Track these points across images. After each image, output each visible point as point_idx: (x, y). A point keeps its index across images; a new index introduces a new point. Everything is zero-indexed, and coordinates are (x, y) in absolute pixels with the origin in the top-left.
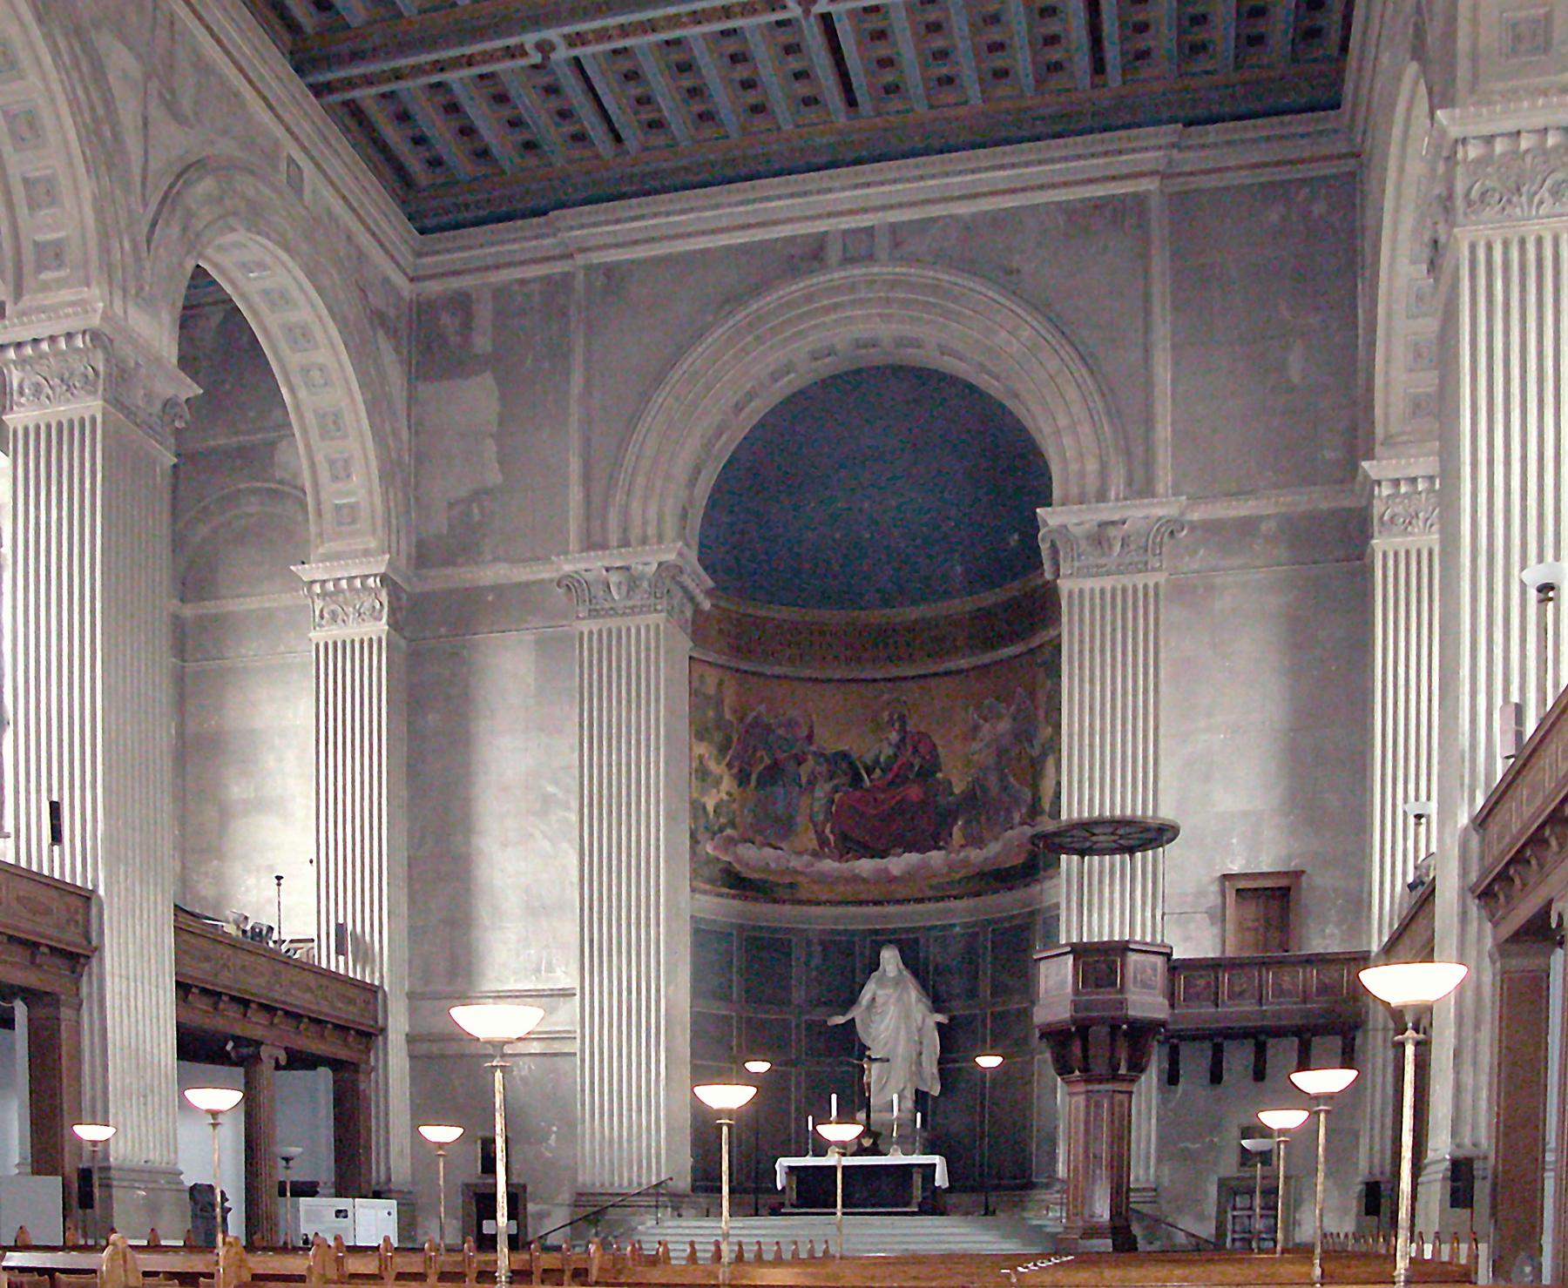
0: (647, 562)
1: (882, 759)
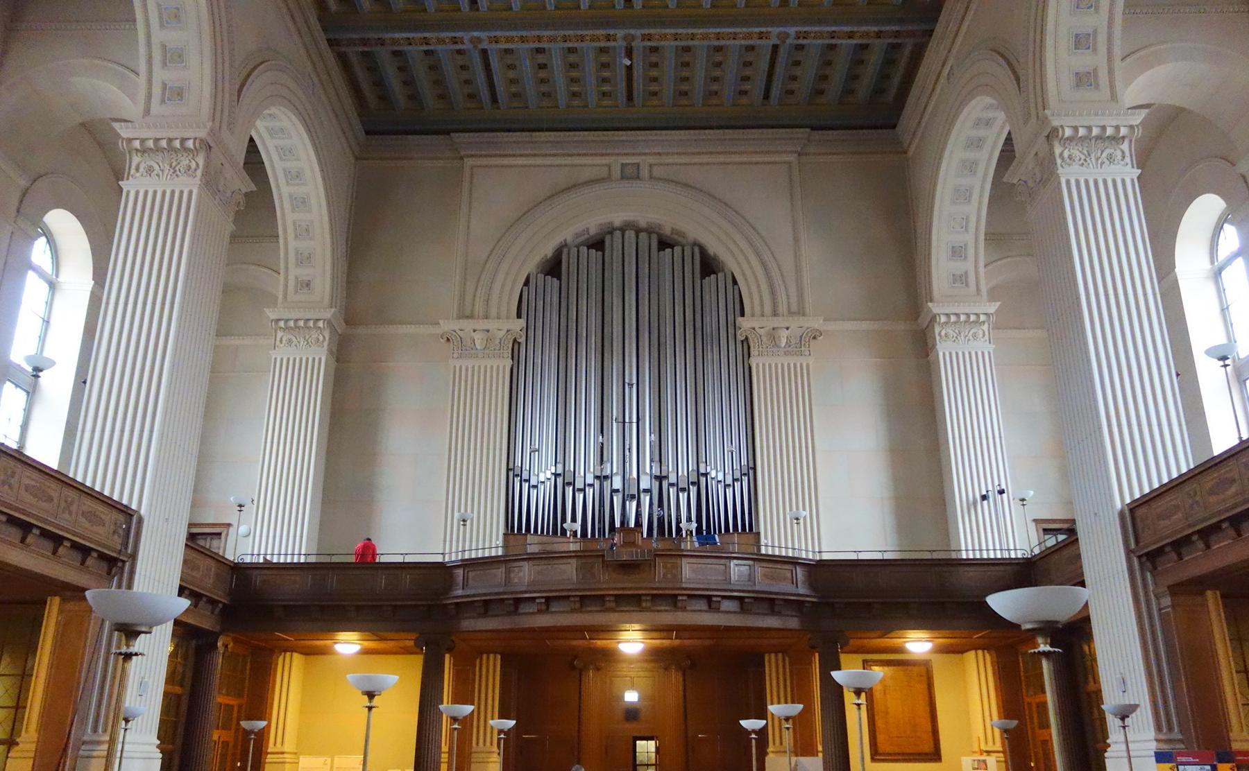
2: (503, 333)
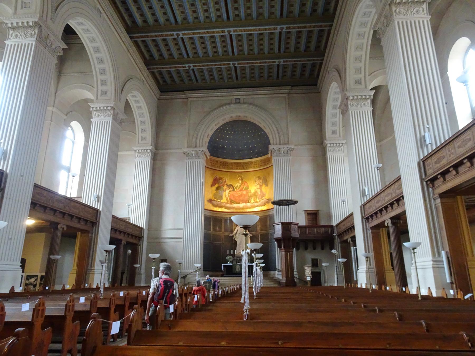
0: (199, 150)
2: (200, 151)
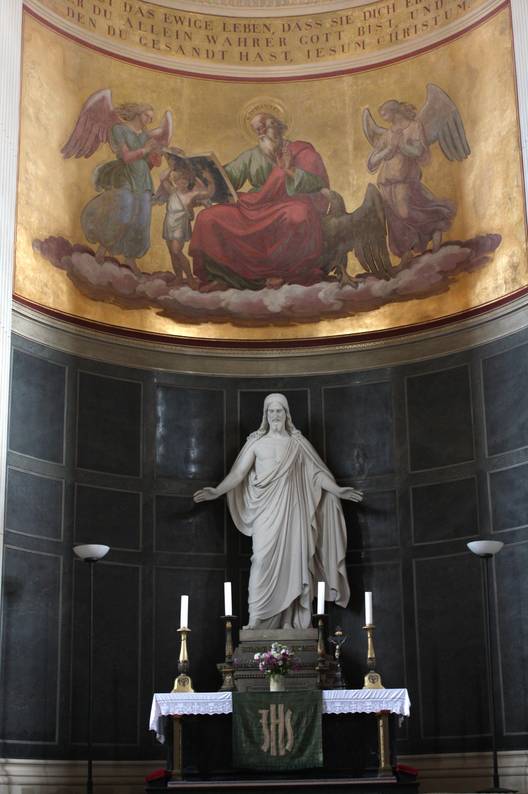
1: (253, 171)
